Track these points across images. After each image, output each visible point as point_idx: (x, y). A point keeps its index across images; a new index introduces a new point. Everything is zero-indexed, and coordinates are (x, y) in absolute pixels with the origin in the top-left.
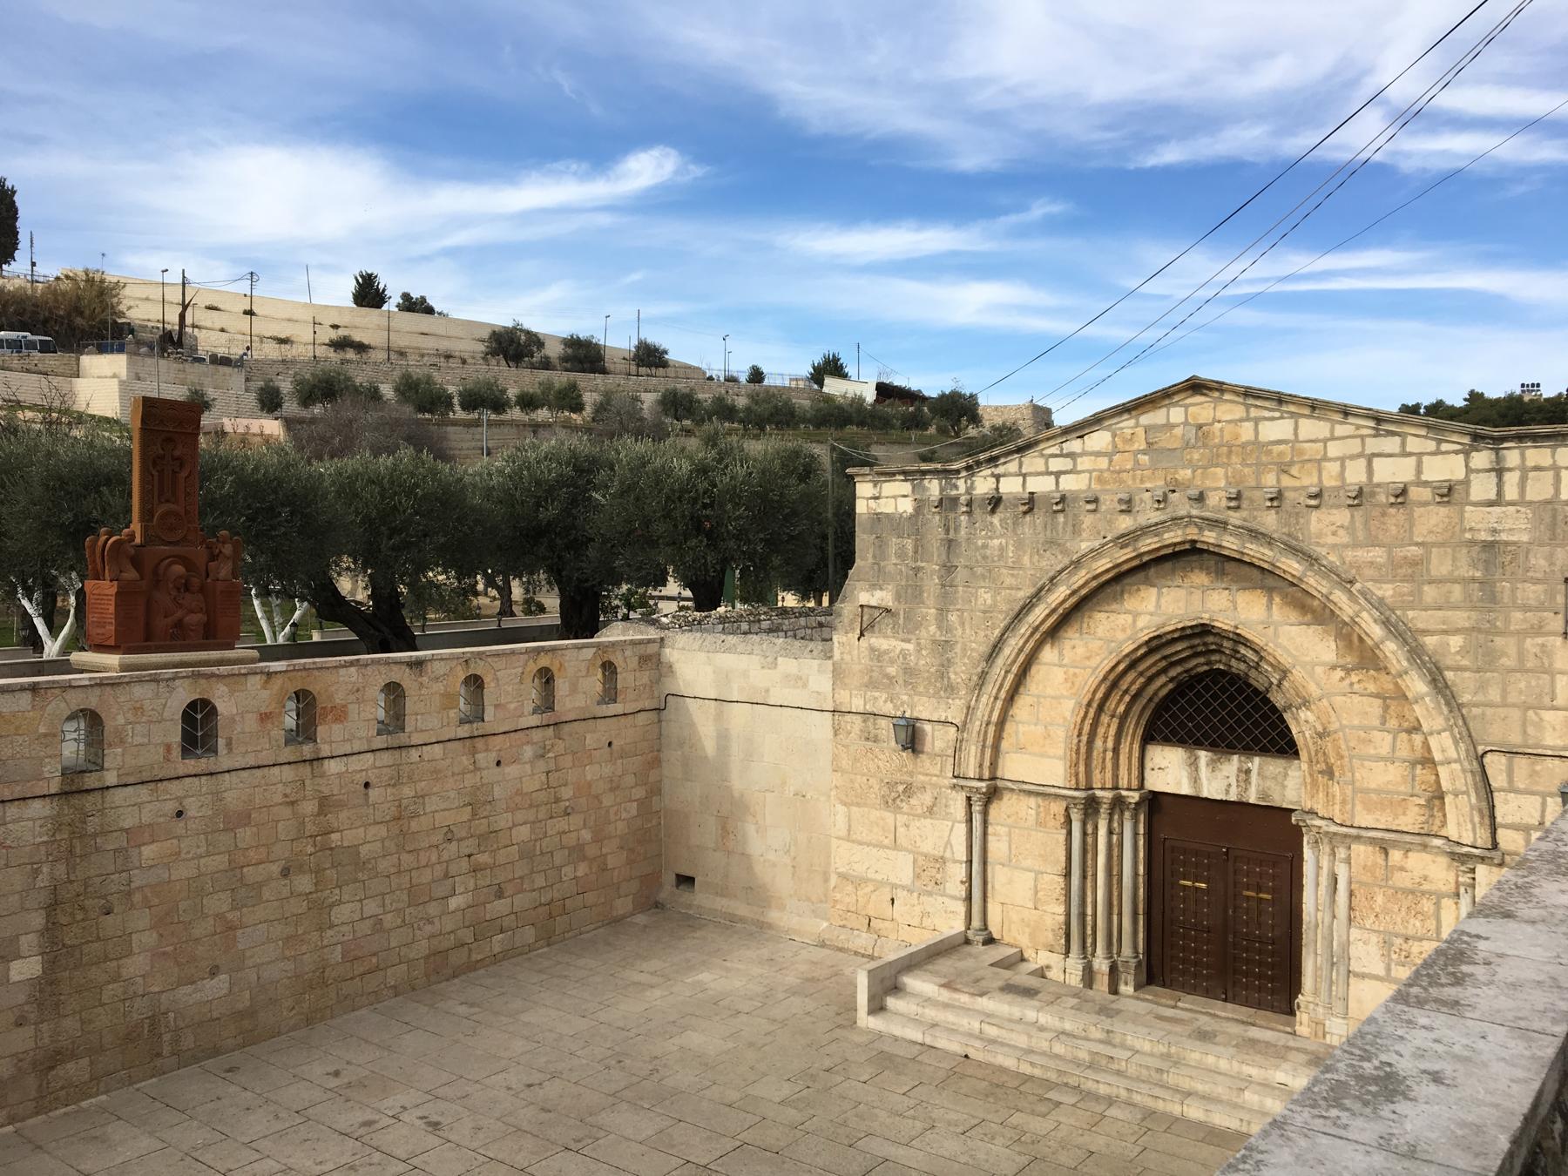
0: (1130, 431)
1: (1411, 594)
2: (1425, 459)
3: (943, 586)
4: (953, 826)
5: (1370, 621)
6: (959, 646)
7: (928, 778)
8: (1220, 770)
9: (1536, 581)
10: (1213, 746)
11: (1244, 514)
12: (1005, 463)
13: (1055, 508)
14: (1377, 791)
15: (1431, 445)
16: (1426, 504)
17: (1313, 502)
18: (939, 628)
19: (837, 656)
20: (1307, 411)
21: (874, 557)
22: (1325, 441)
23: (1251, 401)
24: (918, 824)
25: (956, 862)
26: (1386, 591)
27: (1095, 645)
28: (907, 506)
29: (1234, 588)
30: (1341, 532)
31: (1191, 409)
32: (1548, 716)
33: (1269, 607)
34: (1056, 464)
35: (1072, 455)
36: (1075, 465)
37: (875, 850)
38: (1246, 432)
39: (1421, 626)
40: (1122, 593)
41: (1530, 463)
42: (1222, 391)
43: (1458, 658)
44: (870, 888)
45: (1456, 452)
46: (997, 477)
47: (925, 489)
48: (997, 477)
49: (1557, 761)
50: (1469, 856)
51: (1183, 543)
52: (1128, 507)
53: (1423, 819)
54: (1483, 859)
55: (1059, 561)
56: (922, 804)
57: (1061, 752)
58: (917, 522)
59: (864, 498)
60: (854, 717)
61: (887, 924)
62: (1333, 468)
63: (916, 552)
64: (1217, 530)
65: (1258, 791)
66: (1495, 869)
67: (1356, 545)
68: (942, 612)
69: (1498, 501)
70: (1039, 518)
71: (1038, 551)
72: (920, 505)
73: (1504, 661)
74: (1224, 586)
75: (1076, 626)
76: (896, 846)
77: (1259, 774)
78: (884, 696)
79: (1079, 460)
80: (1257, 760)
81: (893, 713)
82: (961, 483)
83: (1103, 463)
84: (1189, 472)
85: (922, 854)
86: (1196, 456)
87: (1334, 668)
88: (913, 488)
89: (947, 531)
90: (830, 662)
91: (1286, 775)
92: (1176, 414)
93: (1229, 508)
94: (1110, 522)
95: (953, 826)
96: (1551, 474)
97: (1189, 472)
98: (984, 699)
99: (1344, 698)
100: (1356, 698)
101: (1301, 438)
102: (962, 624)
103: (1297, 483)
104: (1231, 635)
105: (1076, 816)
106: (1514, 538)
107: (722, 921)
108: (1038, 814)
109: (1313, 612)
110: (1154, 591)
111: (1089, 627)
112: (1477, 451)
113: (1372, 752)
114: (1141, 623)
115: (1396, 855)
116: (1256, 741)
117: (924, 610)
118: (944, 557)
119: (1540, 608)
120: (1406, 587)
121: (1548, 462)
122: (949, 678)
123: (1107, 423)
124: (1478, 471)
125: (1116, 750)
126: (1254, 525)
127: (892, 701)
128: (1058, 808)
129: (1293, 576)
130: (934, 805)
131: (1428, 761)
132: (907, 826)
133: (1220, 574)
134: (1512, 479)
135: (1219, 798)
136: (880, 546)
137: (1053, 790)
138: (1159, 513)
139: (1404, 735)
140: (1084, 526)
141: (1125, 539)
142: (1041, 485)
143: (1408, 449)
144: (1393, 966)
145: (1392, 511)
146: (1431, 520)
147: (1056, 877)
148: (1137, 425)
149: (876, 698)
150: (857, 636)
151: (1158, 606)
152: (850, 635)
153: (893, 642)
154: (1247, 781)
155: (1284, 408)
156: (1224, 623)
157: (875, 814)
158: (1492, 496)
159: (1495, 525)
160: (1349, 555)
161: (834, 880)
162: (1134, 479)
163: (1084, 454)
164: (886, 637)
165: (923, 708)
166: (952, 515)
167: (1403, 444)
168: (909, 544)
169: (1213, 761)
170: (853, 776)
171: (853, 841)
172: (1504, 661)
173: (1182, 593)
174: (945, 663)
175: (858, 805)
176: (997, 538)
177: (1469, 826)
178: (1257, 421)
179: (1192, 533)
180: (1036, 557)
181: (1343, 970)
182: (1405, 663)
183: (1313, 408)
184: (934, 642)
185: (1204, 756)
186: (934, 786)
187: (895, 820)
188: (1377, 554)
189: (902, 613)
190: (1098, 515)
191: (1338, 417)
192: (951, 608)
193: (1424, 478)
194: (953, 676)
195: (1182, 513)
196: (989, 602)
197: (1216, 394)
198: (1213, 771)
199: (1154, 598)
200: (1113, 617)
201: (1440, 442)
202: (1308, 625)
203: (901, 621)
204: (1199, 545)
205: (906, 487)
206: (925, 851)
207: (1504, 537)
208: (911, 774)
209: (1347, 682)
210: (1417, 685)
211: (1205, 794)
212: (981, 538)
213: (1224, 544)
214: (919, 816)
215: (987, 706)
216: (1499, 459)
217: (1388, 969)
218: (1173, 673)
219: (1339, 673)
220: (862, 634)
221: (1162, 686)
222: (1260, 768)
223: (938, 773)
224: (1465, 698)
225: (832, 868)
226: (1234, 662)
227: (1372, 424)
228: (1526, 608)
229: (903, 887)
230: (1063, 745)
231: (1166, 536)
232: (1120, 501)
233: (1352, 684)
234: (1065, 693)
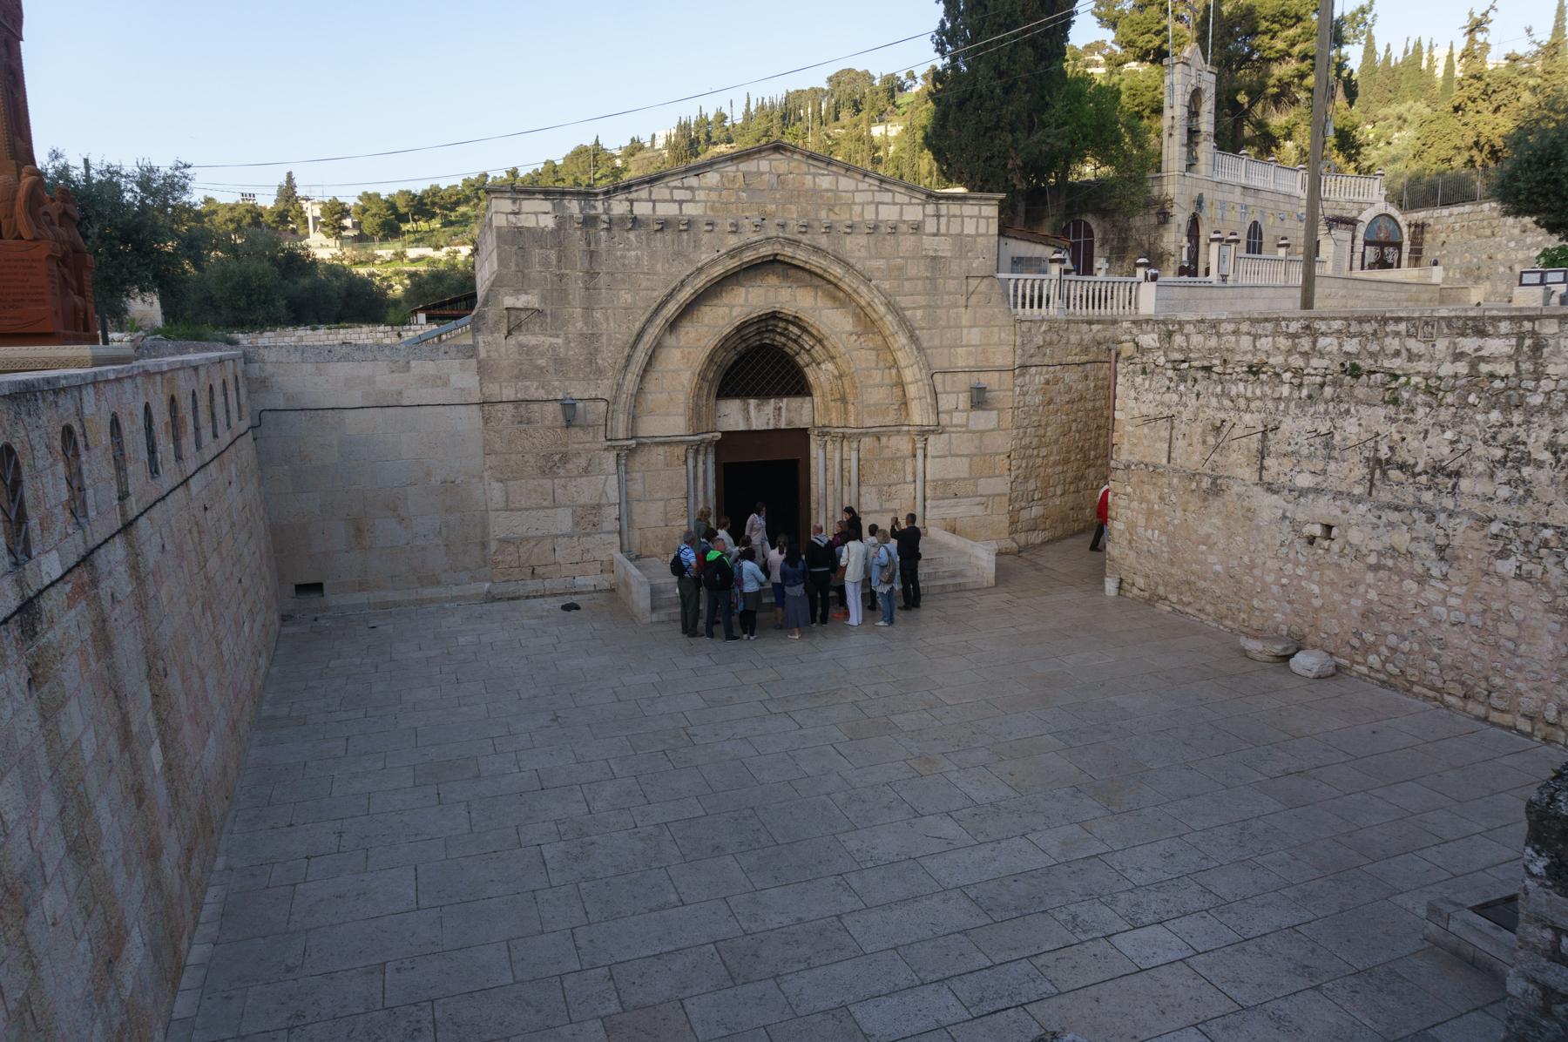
0: (732, 174)
1: (899, 287)
3: (587, 289)
4: (606, 480)
6: (605, 337)
7: (581, 446)
9: (955, 278)
10: (757, 396)
11: (809, 236)
12: (636, 191)
13: (682, 227)
14: (875, 405)
15: (906, 199)
16: (905, 234)
17: (849, 230)
18: (586, 323)
19: (483, 354)
20: (843, 171)
21: (517, 265)
22: (853, 192)
23: (810, 161)
24: (574, 483)
25: (611, 505)
26: (886, 285)
27: (703, 330)
28: (548, 222)
30: (863, 250)
31: (774, 163)
32: (959, 350)
33: (816, 299)
34: (679, 195)
35: (690, 188)
36: (694, 196)
37: (534, 512)
39: (903, 305)
40: (721, 293)
41: (951, 213)
42: (793, 152)
44: (534, 543)
45: (919, 204)
46: (632, 202)
47: (565, 208)
48: (632, 202)
49: (963, 374)
50: (928, 431)
51: (769, 256)
52: (736, 229)
54: (933, 432)
55: (682, 270)
56: (578, 466)
57: (681, 410)
58: (559, 235)
59: (503, 213)
60: (505, 405)
61: (550, 568)
62: (857, 209)
63: (559, 261)
67: (871, 258)
68: (588, 309)
70: (669, 235)
71: (668, 260)
72: (562, 222)
73: (941, 322)
75: (688, 318)
76: (555, 505)
78: (535, 384)
79: (697, 192)
80: (785, 400)
81: (545, 397)
82: (599, 205)
83: (714, 196)
84: (774, 206)
85: (580, 506)
86: (778, 196)
87: (851, 334)
88: (554, 205)
89: (589, 244)
90: (473, 362)
92: (764, 165)
93: (800, 232)
94: (721, 240)
95: (606, 480)
96: (960, 219)
97: (774, 206)
98: (629, 377)
100: (863, 352)
101: (840, 189)
102: (607, 319)
103: (838, 218)
104: (791, 318)
105: (691, 454)
106: (944, 255)
107: (372, 611)
108: (665, 458)
110: (743, 290)
111: (698, 317)
113: (872, 382)
114: (734, 314)
115: (884, 440)
117: (571, 310)
118: (587, 265)
119: (955, 293)
120: (895, 283)
121: (958, 213)
122: (597, 363)
123: (716, 167)
124: (929, 216)
126: (814, 244)
127: (543, 388)
128: (680, 450)
129: (835, 277)
130: (589, 465)
131: (901, 384)
132: (565, 487)
133: (786, 277)
134: (943, 220)
135: (763, 428)
136: (523, 256)
137: (679, 438)
138: (755, 234)
139: (887, 371)
140: (703, 242)
141: (733, 253)
142: (666, 210)
143: (896, 201)
145: (888, 237)
146: (908, 242)
147: (681, 500)
148: (738, 170)
149: (527, 387)
150: (503, 336)
151: (746, 299)
152: (496, 335)
153: (542, 338)
154: (780, 415)
155: (830, 168)
156: (789, 310)
157: (532, 483)
158: (935, 231)
160: (868, 263)
161: (494, 546)
162: (737, 209)
163: (700, 188)
164: (534, 334)
165: (577, 390)
166: (592, 231)
167: (894, 197)
168: (553, 254)
169: (758, 405)
170: (507, 456)
171: (512, 510)
172: (941, 322)
173: (762, 290)
174: (593, 351)
175: (515, 479)
176: (634, 250)
178: (815, 175)
179: (777, 249)
180: (667, 265)
183: (847, 170)
184: (582, 335)
185: (753, 402)
186: (588, 451)
187: (553, 484)
188: (881, 263)
189: (549, 312)
190: (712, 234)
191: (860, 177)
192: (596, 307)
193: (904, 218)
194: (600, 362)
195: (774, 234)
196: (629, 301)
197: (789, 154)
199: (743, 295)
200: (715, 309)
201: (911, 197)
203: (549, 320)
204: (778, 258)
205: (547, 206)
206: (582, 502)
207: (940, 254)
208: (566, 445)
210: (902, 340)
211: (754, 427)
212: (620, 250)
213: (798, 257)
214: (575, 477)
215: (631, 379)
216: (938, 210)
217: (881, 505)
218: (739, 348)
219: (854, 337)
220: (509, 333)
221: (732, 356)
223: (590, 440)
224: (925, 345)
225: (492, 536)
226: (778, 338)
227: (877, 183)
228: (949, 293)
229: (563, 536)
230: (682, 405)
231: (761, 250)
232: (731, 225)
234: (682, 366)
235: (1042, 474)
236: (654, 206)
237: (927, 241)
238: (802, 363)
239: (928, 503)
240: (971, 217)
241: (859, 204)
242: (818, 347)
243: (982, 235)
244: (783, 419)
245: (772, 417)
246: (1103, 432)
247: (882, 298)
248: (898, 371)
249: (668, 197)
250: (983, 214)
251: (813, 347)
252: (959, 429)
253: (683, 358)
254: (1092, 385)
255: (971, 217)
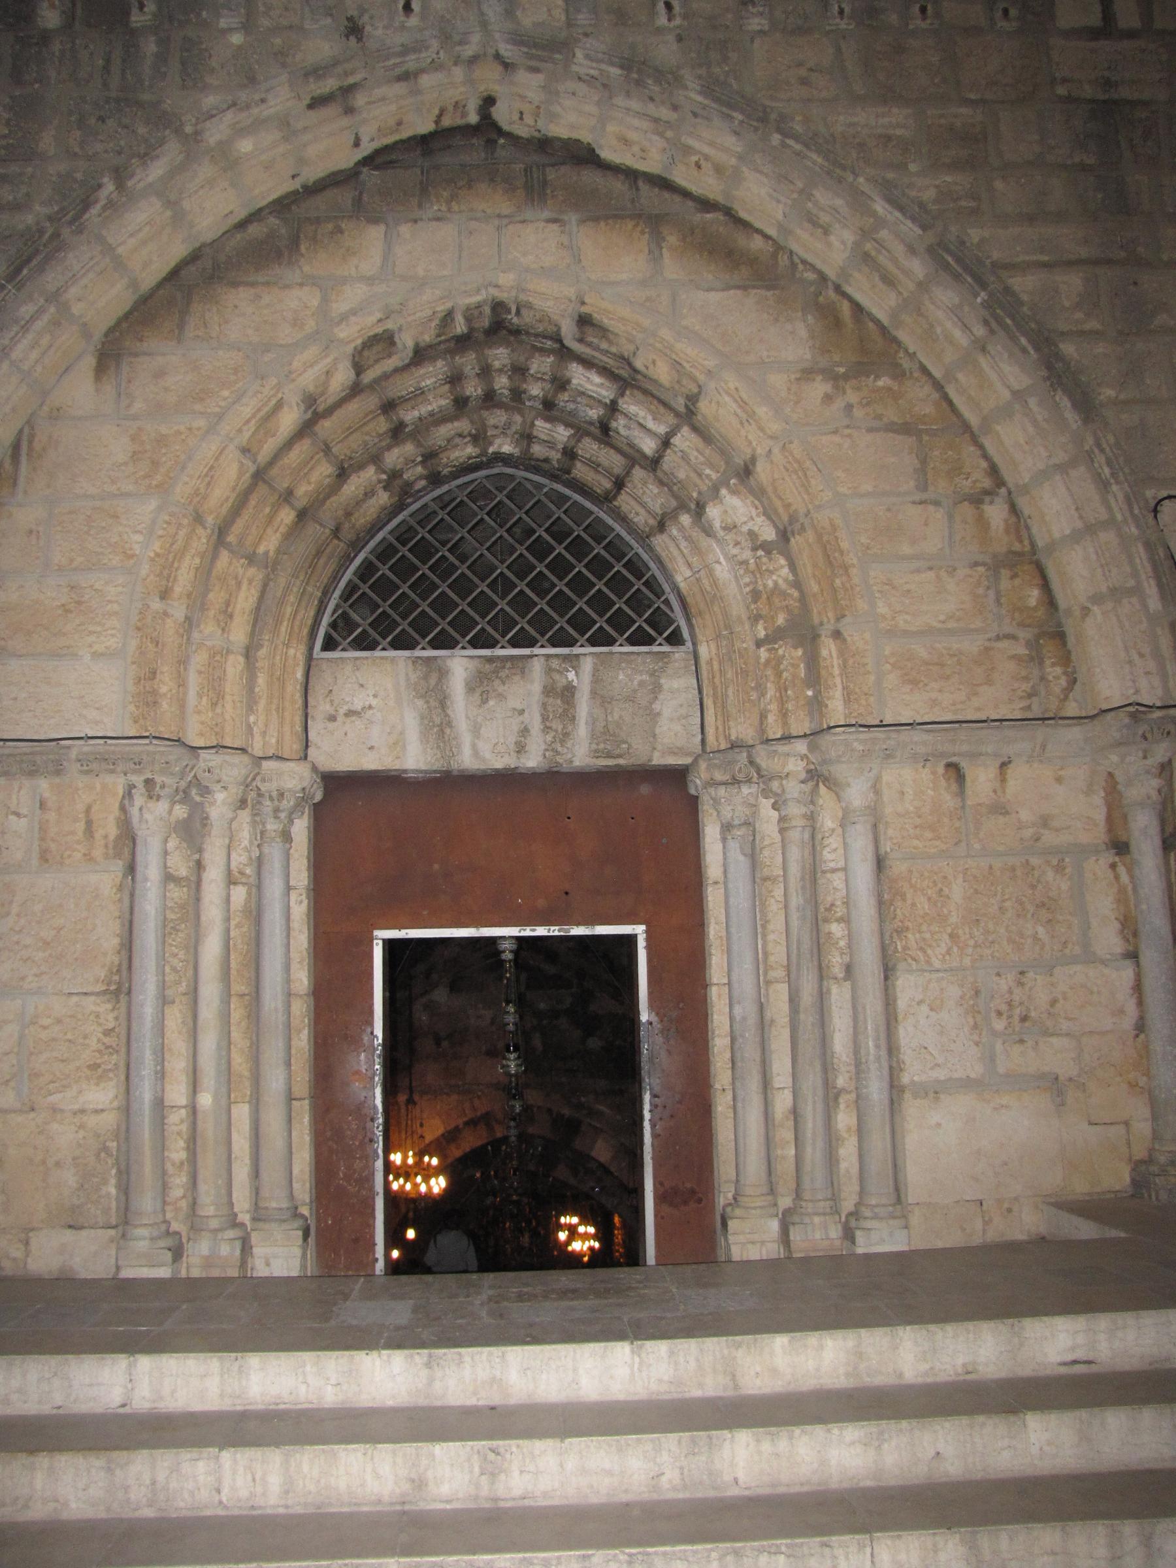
5: (899, 249)
8: (502, 697)
29: (573, 218)
43: (1079, 315)
53: (1026, 686)
65: (593, 736)
74: (546, 214)
77: (594, 693)
91: (657, 689)
99: (837, 439)
109: (752, 261)
110: (375, 233)
115: (981, 779)
116: (581, 624)
125: (249, 653)
135: (499, 764)
139: (967, 509)
144: (999, 1047)
154: (569, 716)
159: (1107, 74)
173: (447, 232)
177: (1152, 665)
181: (876, 1089)
182: (980, 331)
198: (485, 701)
202: (744, 288)
209: (839, 403)
217: (990, 1059)
219: (820, 387)
222: (596, 680)
226: (542, 427)
233: (849, 407)
238: (641, 518)
242: (685, 440)
244: (582, 731)
245: (536, 725)
247: (910, 228)
248: (1014, 509)
251: (666, 443)
253: (135, 456)
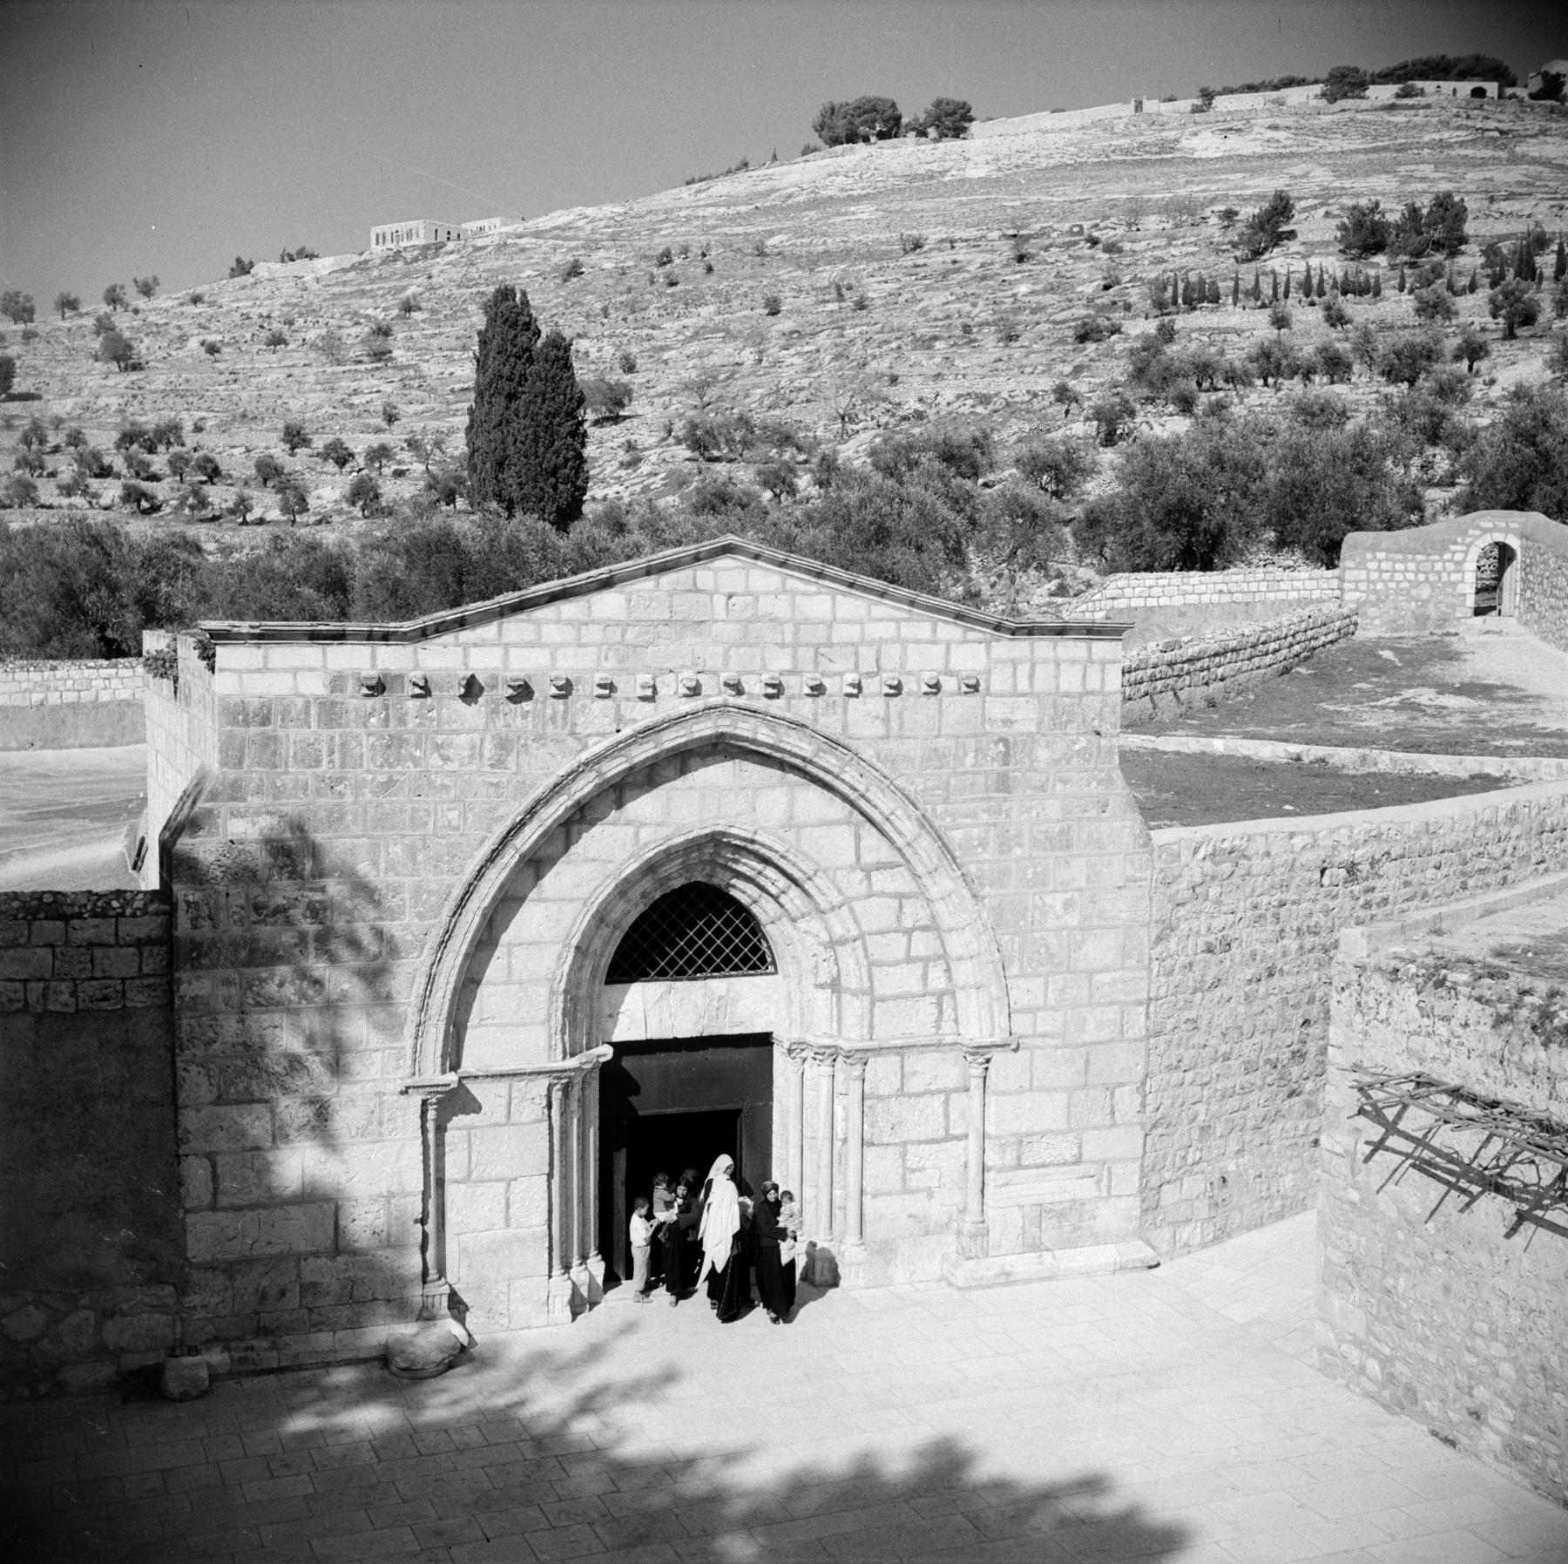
2: (953, 646)
11: (781, 702)
28: (315, 686)
30: (878, 722)
38: (780, 607)
44: (262, 1269)
46: (466, 647)
48: (466, 647)
64: (753, 720)
66: (1012, 1055)
69: (1015, 694)
83: (615, 634)
96: (1052, 666)
101: (839, 616)
105: (557, 1095)
112: (998, 640)
114: (645, 834)
121: (1050, 654)
134: (1023, 671)
145: (924, 699)
146: (956, 707)
179: (723, 725)
221: (630, 912)
231: (695, 728)
235: (1201, 1117)
236: (506, 654)
237: (997, 709)
239: (990, 1176)
240: (1074, 662)
241: (871, 644)
243: (1092, 693)
246: (1315, 1030)
249: (532, 637)
250: (1094, 657)
252: (1051, 1041)
254: (1294, 946)
255: (1074, 662)
